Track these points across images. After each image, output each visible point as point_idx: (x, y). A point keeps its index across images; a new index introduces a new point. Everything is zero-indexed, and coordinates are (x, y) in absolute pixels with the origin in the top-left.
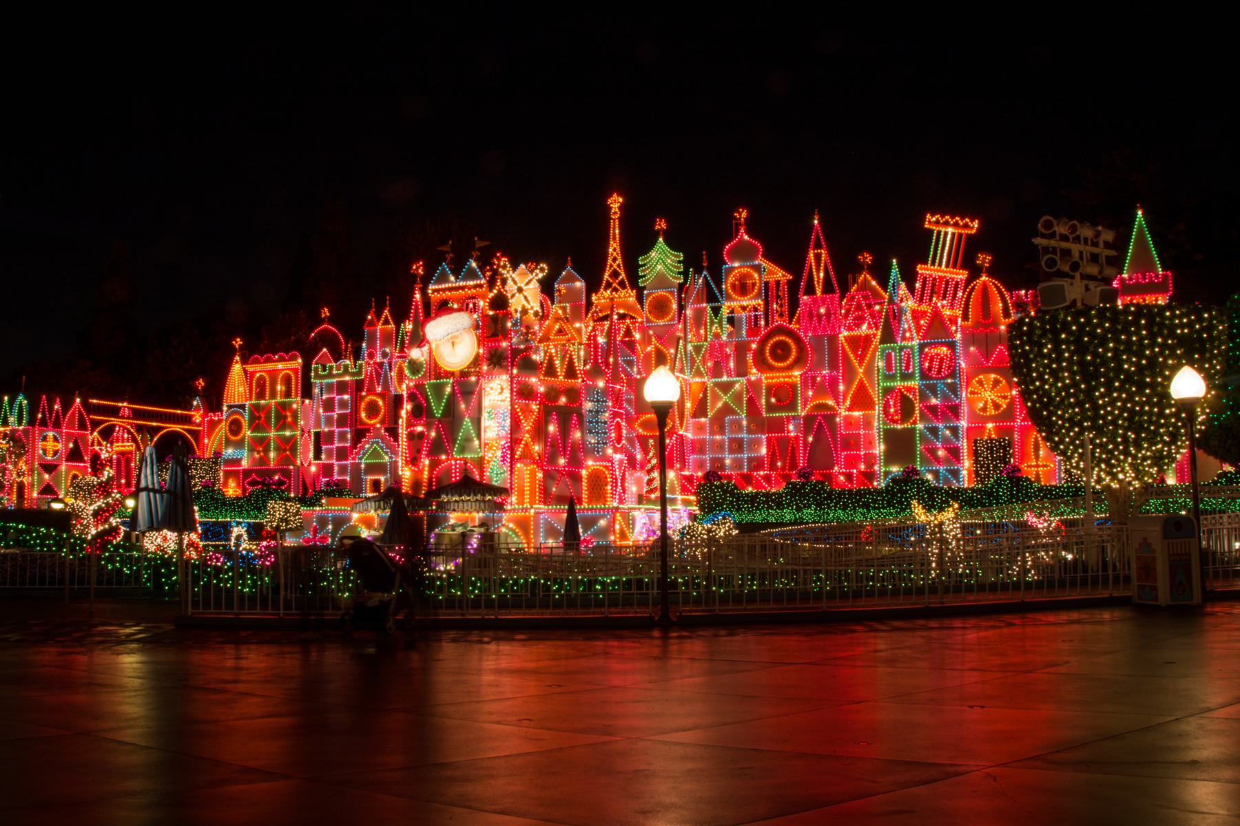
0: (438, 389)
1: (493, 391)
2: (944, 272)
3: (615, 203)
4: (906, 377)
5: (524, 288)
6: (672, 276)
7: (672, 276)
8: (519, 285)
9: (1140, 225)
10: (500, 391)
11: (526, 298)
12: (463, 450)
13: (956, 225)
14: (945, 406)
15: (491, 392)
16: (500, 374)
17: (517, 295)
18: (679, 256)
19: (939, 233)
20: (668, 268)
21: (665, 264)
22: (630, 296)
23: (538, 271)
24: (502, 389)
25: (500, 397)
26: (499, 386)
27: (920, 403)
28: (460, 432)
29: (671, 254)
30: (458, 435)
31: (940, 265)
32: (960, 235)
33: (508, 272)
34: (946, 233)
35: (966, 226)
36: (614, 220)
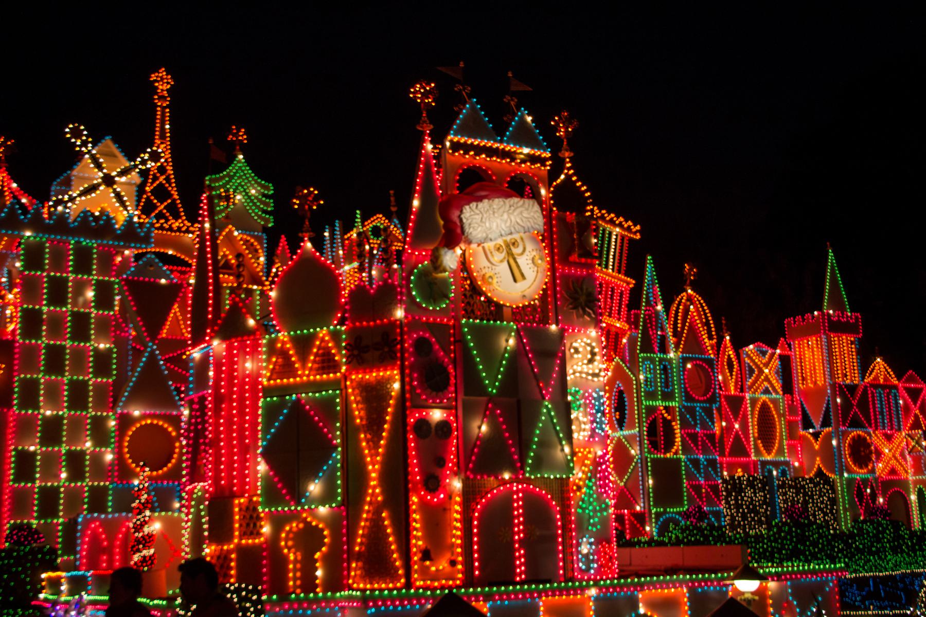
0: (486, 338)
1: (580, 356)
2: (608, 275)
3: (162, 81)
4: (668, 396)
5: (117, 179)
6: (256, 214)
7: (256, 214)
8: (105, 171)
9: (832, 263)
10: (589, 356)
11: (118, 196)
12: (538, 464)
13: (620, 225)
14: (705, 435)
15: (576, 356)
16: (586, 326)
17: (102, 188)
18: (267, 188)
19: (604, 230)
20: (255, 204)
21: (247, 194)
22: (188, 231)
23: (146, 157)
24: (593, 354)
25: (591, 369)
26: (589, 348)
27: (681, 429)
28: (535, 426)
29: (256, 182)
30: (532, 434)
31: (607, 267)
32: (623, 237)
33: (84, 144)
34: (610, 234)
35: (628, 229)
36: (163, 108)
